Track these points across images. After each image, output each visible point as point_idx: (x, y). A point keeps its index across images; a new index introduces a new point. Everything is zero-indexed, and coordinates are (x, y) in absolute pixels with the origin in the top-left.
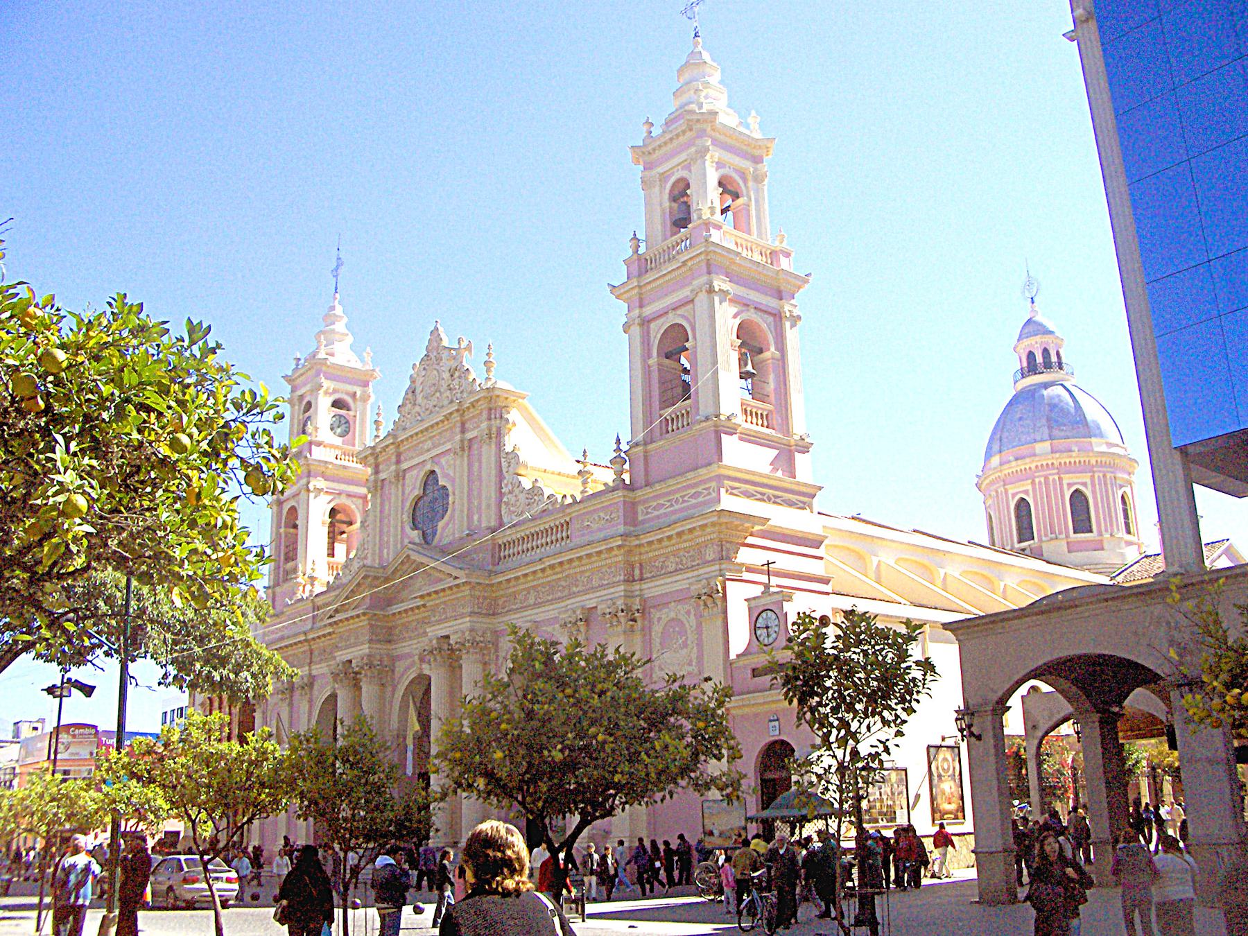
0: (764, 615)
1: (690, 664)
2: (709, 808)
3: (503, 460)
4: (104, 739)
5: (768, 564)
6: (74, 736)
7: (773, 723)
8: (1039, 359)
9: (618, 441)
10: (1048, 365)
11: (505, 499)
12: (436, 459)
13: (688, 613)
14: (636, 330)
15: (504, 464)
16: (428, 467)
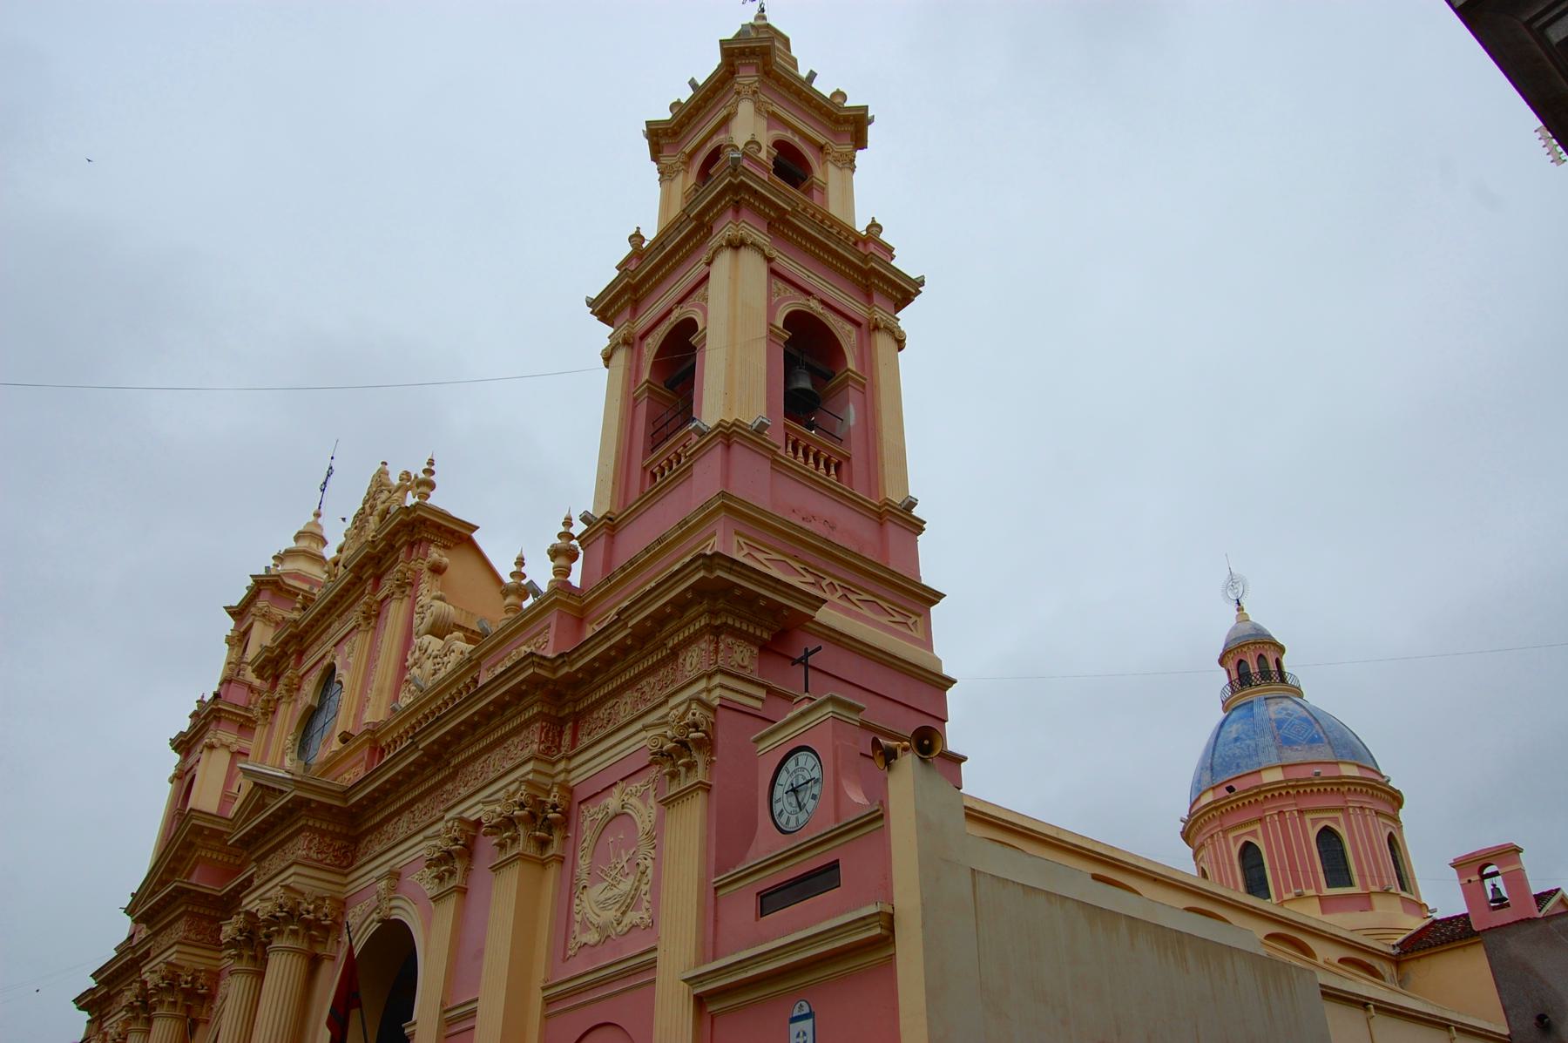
0: (791, 764)
3: (416, 616)
7: (796, 1027)
8: (1253, 667)
10: (1265, 675)
11: (408, 677)
14: (621, 356)
15: (416, 619)
16: (326, 662)
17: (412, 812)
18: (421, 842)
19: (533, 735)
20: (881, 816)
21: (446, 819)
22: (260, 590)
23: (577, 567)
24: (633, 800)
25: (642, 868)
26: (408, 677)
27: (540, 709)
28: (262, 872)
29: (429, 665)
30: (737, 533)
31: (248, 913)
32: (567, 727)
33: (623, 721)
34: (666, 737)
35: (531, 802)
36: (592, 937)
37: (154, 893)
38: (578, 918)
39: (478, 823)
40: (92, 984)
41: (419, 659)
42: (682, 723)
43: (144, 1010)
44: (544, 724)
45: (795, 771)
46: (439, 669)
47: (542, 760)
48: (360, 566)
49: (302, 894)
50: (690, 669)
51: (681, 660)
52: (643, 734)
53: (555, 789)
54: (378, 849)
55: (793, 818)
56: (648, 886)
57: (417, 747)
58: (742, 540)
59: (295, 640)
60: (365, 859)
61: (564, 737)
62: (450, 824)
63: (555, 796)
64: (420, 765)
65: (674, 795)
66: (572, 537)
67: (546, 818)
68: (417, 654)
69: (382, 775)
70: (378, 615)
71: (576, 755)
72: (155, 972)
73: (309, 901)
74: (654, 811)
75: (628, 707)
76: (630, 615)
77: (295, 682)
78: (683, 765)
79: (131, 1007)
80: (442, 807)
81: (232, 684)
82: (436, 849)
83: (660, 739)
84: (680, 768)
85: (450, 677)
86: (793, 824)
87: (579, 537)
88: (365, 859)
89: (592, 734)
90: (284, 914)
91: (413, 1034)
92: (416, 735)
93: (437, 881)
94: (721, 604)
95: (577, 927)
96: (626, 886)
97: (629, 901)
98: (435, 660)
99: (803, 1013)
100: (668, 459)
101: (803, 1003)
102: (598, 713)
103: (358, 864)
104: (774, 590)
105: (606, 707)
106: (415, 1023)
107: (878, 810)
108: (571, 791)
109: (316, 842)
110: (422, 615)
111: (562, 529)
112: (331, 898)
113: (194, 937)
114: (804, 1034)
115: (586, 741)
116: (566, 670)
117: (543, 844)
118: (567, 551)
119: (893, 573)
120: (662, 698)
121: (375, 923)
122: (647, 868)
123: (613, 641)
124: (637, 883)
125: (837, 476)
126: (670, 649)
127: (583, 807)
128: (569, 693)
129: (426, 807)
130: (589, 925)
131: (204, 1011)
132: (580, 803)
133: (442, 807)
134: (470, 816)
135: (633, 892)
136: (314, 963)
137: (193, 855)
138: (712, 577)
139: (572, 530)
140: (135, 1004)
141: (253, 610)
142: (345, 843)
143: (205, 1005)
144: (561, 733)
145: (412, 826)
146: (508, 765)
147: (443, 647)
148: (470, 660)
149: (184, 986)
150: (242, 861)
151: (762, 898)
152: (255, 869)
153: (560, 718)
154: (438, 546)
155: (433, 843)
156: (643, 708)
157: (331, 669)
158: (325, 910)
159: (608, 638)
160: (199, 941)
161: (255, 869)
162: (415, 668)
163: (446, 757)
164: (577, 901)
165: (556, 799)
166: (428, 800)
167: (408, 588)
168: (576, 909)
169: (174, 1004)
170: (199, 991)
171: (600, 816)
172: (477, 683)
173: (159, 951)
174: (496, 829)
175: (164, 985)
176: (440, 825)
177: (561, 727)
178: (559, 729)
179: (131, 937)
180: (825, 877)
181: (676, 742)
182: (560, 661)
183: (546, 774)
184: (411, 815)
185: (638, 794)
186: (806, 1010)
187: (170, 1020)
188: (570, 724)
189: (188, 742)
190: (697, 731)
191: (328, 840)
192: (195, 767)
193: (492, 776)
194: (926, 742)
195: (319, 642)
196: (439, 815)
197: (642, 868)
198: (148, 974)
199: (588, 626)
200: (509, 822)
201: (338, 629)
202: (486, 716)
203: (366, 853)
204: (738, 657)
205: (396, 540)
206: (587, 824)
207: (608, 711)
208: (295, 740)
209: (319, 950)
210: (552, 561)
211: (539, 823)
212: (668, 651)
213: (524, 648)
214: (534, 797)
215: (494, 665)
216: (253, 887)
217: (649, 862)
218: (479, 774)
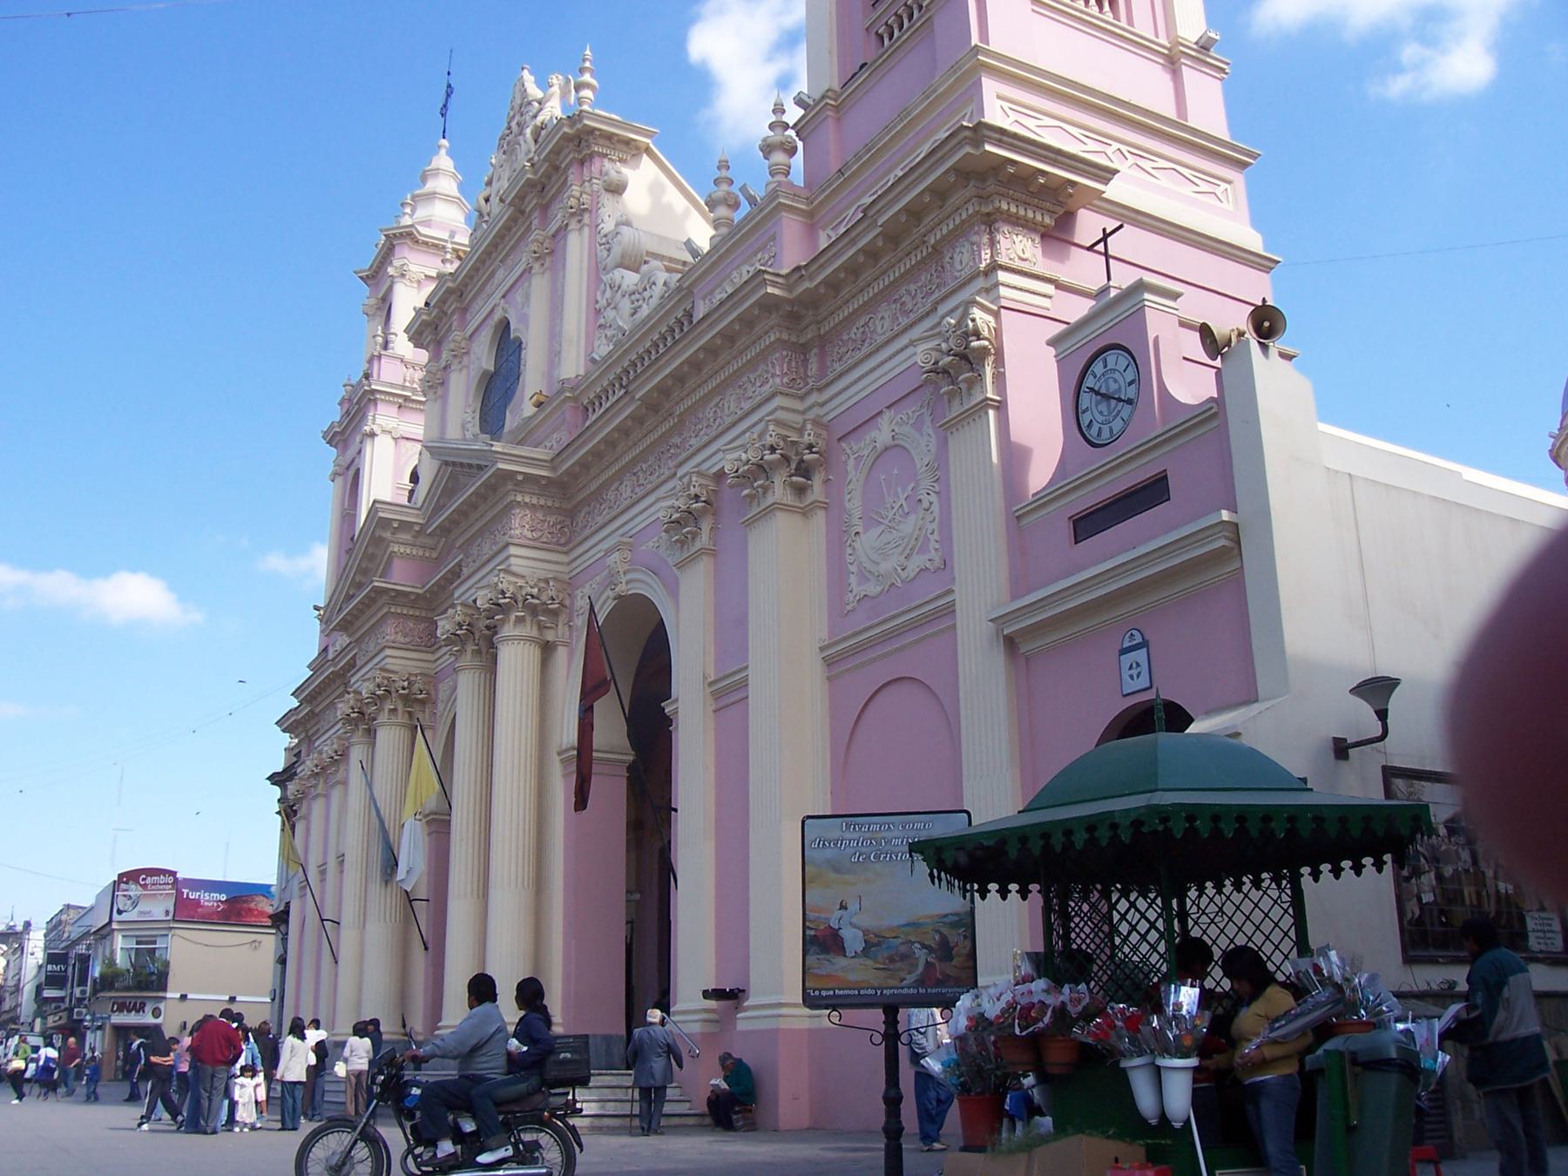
0: (1098, 367)
1: (923, 549)
2: (823, 843)
4: (185, 891)
5: (1104, 239)
6: (145, 887)
9: (779, 109)
12: (509, 295)
13: (918, 425)
16: (497, 316)
17: (635, 474)
18: (654, 503)
19: (773, 367)
20: (1215, 414)
21: (678, 475)
22: (394, 246)
23: (798, 160)
24: (907, 429)
25: (925, 504)
26: (602, 321)
27: (778, 336)
28: (470, 559)
29: (626, 305)
30: (999, 97)
31: (464, 605)
32: (813, 352)
33: (880, 340)
34: (940, 351)
35: (782, 444)
36: (873, 589)
37: (349, 598)
38: (853, 568)
39: (720, 476)
40: (295, 703)
41: (613, 298)
42: (958, 333)
43: (364, 722)
44: (785, 353)
45: (1103, 374)
46: (640, 307)
47: (787, 395)
48: (521, 197)
49: (523, 577)
50: (959, 267)
51: (947, 259)
52: (910, 350)
53: (809, 426)
54: (600, 520)
55: (1106, 429)
56: (935, 526)
57: (633, 397)
58: (1006, 105)
60: (587, 532)
61: (810, 367)
62: (686, 480)
63: (809, 435)
64: (638, 419)
65: (957, 417)
66: (786, 127)
67: (802, 461)
68: (608, 293)
69: (595, 434)
70: (552, 253)
71: (828, 385)
72: (369, 679)
73: (532, 583)
74: (933, 440)
75: (887, 324)
76: (879, 211)
77: (463, 345)
78: (965, 380)
79: (347, 719)
80: (671, 464)
81: (383, 360)
82: (673, 510)
83: (933, 353)
84: (960, 386)
85: (657, 313)
86: (1106, 434)
87: (795, 125)
88: (587, 532)
89: (845, 359)
90: (508, 600)
91: (676, 711)
92: (630, 382)
93: (679, 545)
94: (991, 186)
95: (853, 579)
96: (909, 526)
97: (913, 542)
98: (633, 297)
99: (1134, 642)
100: (896, 14)
101: (1134, 632)
102: (849, 334)
103: (579, 539)
104: (1054, 163)
105: (857, 325)
106: (677, 700)
107: (1211, 408)
108: (826, 427)
109: (528, 519)
110: (607, 246)
111: (773, 118)
112: (555, 579)
113: (402, 640)
114: (1138, 665)
115: (838, 368)
116: (807, 285)
117: (800, 491)
118: (783, 144)
119: (1195, 132)
120: (928, 307)
121: (610, 601)
122: (931, 503)
123: (861, 244)
124: (921, 522)
125: (1113, 13)
126: (933, 247)
127: (844, 445)
128: (810, 313)
129: (650, 466)
130: (867, 574)
132: (839, 440)
133: (671, 464)
134: (708, 469)
135: (917, 532)
136: (547, 649)
137: (385, 552)
138: (978, 153)
139: (785, 118)
140: (352, 715)
141: (391, 271)
142: (560, 518)
143: (427, 711)
144: (805, 361)
145: (637, 490)
146: (747, 406)
147: (641, 280)
148: (679, 289)
149: (401, 692)
151: (1074, 522)
152: (461, 556)
153: (802, 345)
154: (612, 160)
155: (669, 503)
156: (904, 321)
157: (505, 326)
158: (553, 593)
159: (853, 242)
160: (408, 643)
161: (461, 556)
162: (609, 309)
163: (667, 406)
164: (849, 551)
165: (811, 437)
166: (651, 459)
167: (586, 216)
168: (850, 559)
171: (866, 452)
172: (692, 316)
173: (366, 659)
174: (745, 478)
176: (670, 485)
177: (805, 355)
178: (802, 357)
179: (325, 650)
180: (1153, 492)
181: (953, 355)
182: (797, 276)
183: (794, 411)
184: (635, 478)
185: (912, 421)
186: (1138, 639)
188: (815, 350)
190: (979, 339)
191: (540, 515)
192: (357, 460)
193: (728, 421)
194: (1267, 324)
195: (484, 295)
196: (667, 473)
197: (925, 504)
198: (359, 683)
199: (821, 232)
200: (762, 469)
201: (503, 278)
202: (711, 351)
203: (585, 527)
204: (1019, 248)
205: (561, 158)
206: (851, 462)
207: (861, 330)
208: (474, 412)
209: (550, 636)
210: (766, 158)
211: (793, 466)
212: (930, 250)
213: (745, 268)
214: (785, 438)
215: (712, 293)
216: (462, 578)
217: (933, 498)
218: (712, 420)
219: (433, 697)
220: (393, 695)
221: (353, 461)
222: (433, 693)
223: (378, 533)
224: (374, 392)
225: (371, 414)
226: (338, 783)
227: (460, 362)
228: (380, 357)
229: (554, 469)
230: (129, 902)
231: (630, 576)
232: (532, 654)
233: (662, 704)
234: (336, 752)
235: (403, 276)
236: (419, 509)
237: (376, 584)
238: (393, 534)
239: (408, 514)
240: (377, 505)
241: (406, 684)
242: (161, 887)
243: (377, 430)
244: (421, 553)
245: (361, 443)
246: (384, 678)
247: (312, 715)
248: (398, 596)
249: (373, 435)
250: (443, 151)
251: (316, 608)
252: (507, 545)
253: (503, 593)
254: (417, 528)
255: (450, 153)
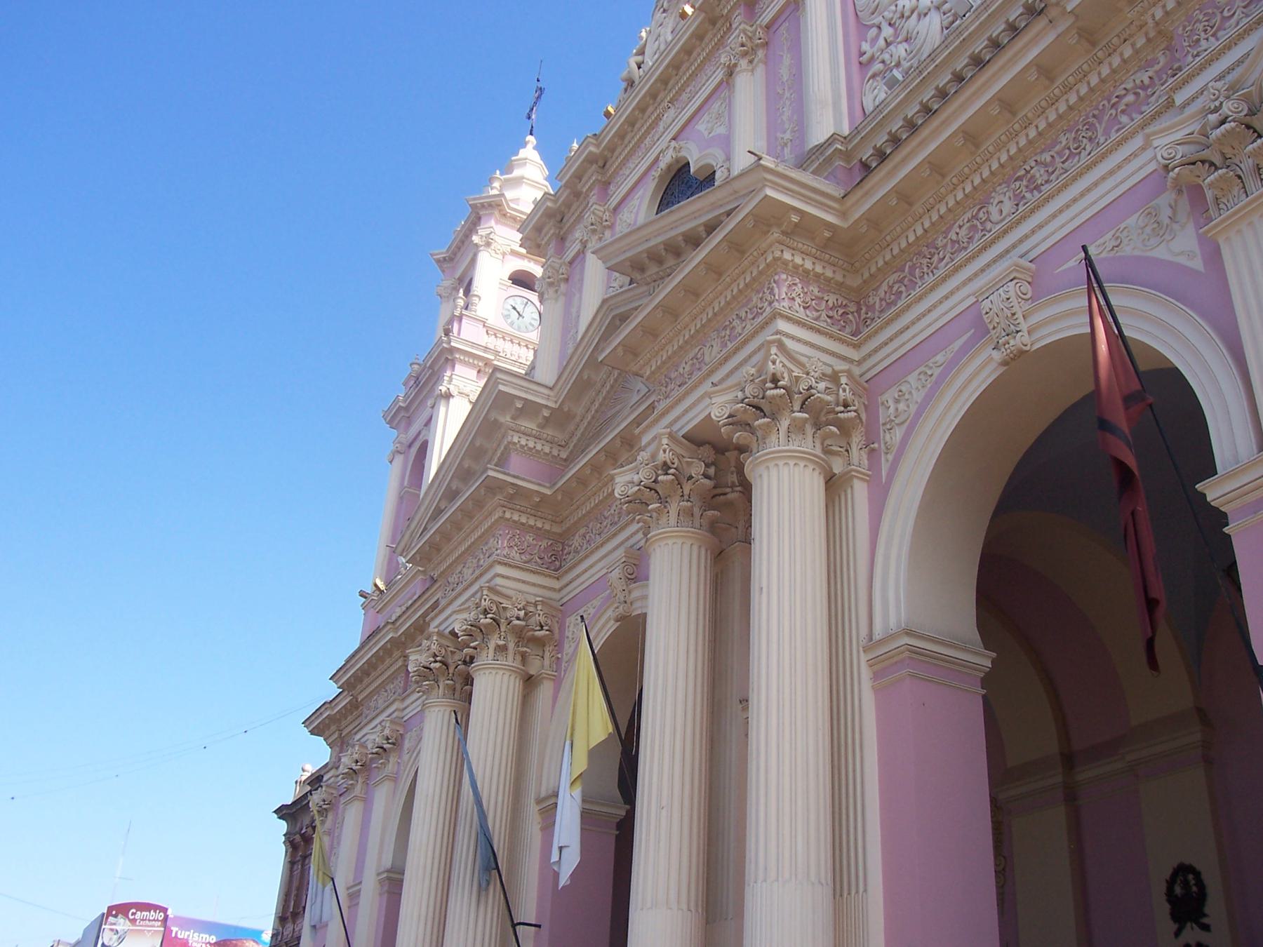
4: (174, 929)
6: (133, 921)
22: (479, 219)
40: (333, 690)
49: (801, 365)
59: (594, 167)
109: (798, 289)
131: (547, 662)
141: (475, 239)
143: (547, 655)
150: (571, 452)
169: (502, 649)
170: (537, 633)
175: (488, 621)
187: (501, 672)
189: (407, 409)
209: (838, 467)
219: (557, 636)
220: (503, 629)
221: (419, 433)
222: (556, 631)
223: (493, 416)
224: (453, 350)
225: (448, 373)
226: (387, 777)
227: (600, 239)
228: (460, 318)
229: (843, 215)
230: (115, 937)
231: (1034, 320)
232: (813, 483)
233: (1196, 487)
234: (388, 739)
235: (488, 244)
236: (551, 389)
237: (491, 473)
238: (514, 418)
239: (536, 393)
240: (499, 375)
241: (522, 613)
242: (151, 923)
243: (454, 391)
244: (547, 450)
245: (433, 407)
246: (492, 601)
247: (354, 706)
248: (517, 495)
249: (448, 396)
250: (530, 146)
251: (363, 594)
252: (775, 315)
253: (775, 380)
254: (546, 413)
255: (535, 148)
